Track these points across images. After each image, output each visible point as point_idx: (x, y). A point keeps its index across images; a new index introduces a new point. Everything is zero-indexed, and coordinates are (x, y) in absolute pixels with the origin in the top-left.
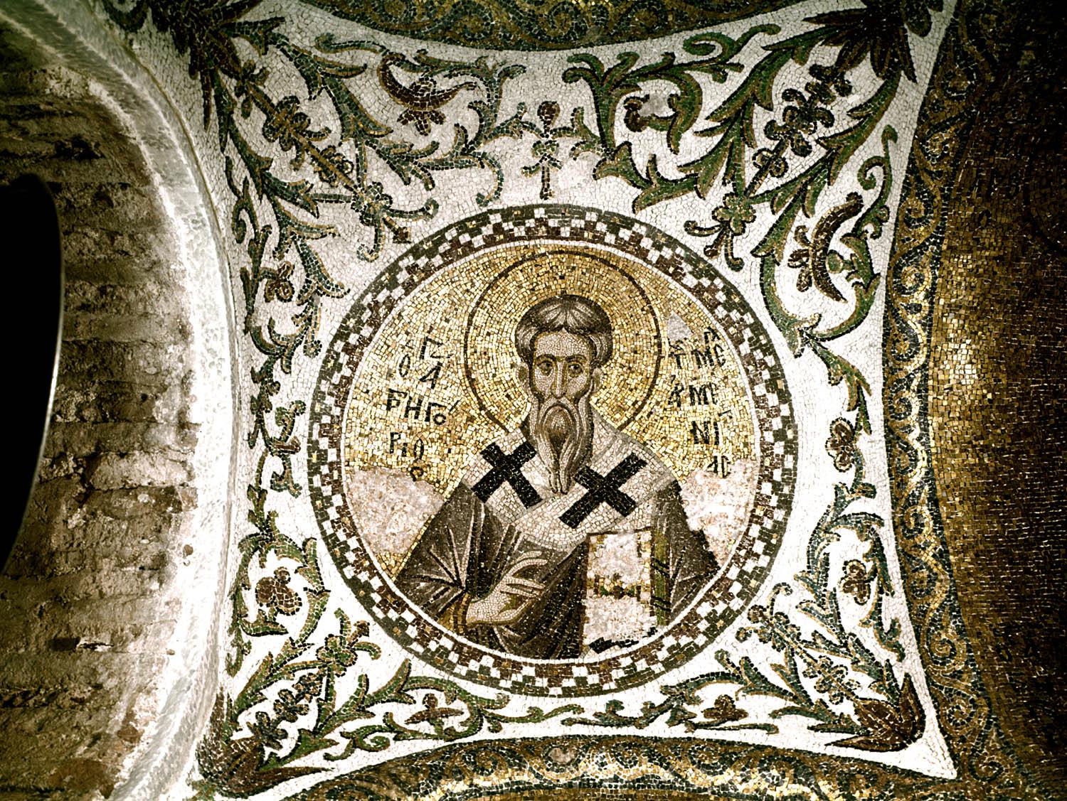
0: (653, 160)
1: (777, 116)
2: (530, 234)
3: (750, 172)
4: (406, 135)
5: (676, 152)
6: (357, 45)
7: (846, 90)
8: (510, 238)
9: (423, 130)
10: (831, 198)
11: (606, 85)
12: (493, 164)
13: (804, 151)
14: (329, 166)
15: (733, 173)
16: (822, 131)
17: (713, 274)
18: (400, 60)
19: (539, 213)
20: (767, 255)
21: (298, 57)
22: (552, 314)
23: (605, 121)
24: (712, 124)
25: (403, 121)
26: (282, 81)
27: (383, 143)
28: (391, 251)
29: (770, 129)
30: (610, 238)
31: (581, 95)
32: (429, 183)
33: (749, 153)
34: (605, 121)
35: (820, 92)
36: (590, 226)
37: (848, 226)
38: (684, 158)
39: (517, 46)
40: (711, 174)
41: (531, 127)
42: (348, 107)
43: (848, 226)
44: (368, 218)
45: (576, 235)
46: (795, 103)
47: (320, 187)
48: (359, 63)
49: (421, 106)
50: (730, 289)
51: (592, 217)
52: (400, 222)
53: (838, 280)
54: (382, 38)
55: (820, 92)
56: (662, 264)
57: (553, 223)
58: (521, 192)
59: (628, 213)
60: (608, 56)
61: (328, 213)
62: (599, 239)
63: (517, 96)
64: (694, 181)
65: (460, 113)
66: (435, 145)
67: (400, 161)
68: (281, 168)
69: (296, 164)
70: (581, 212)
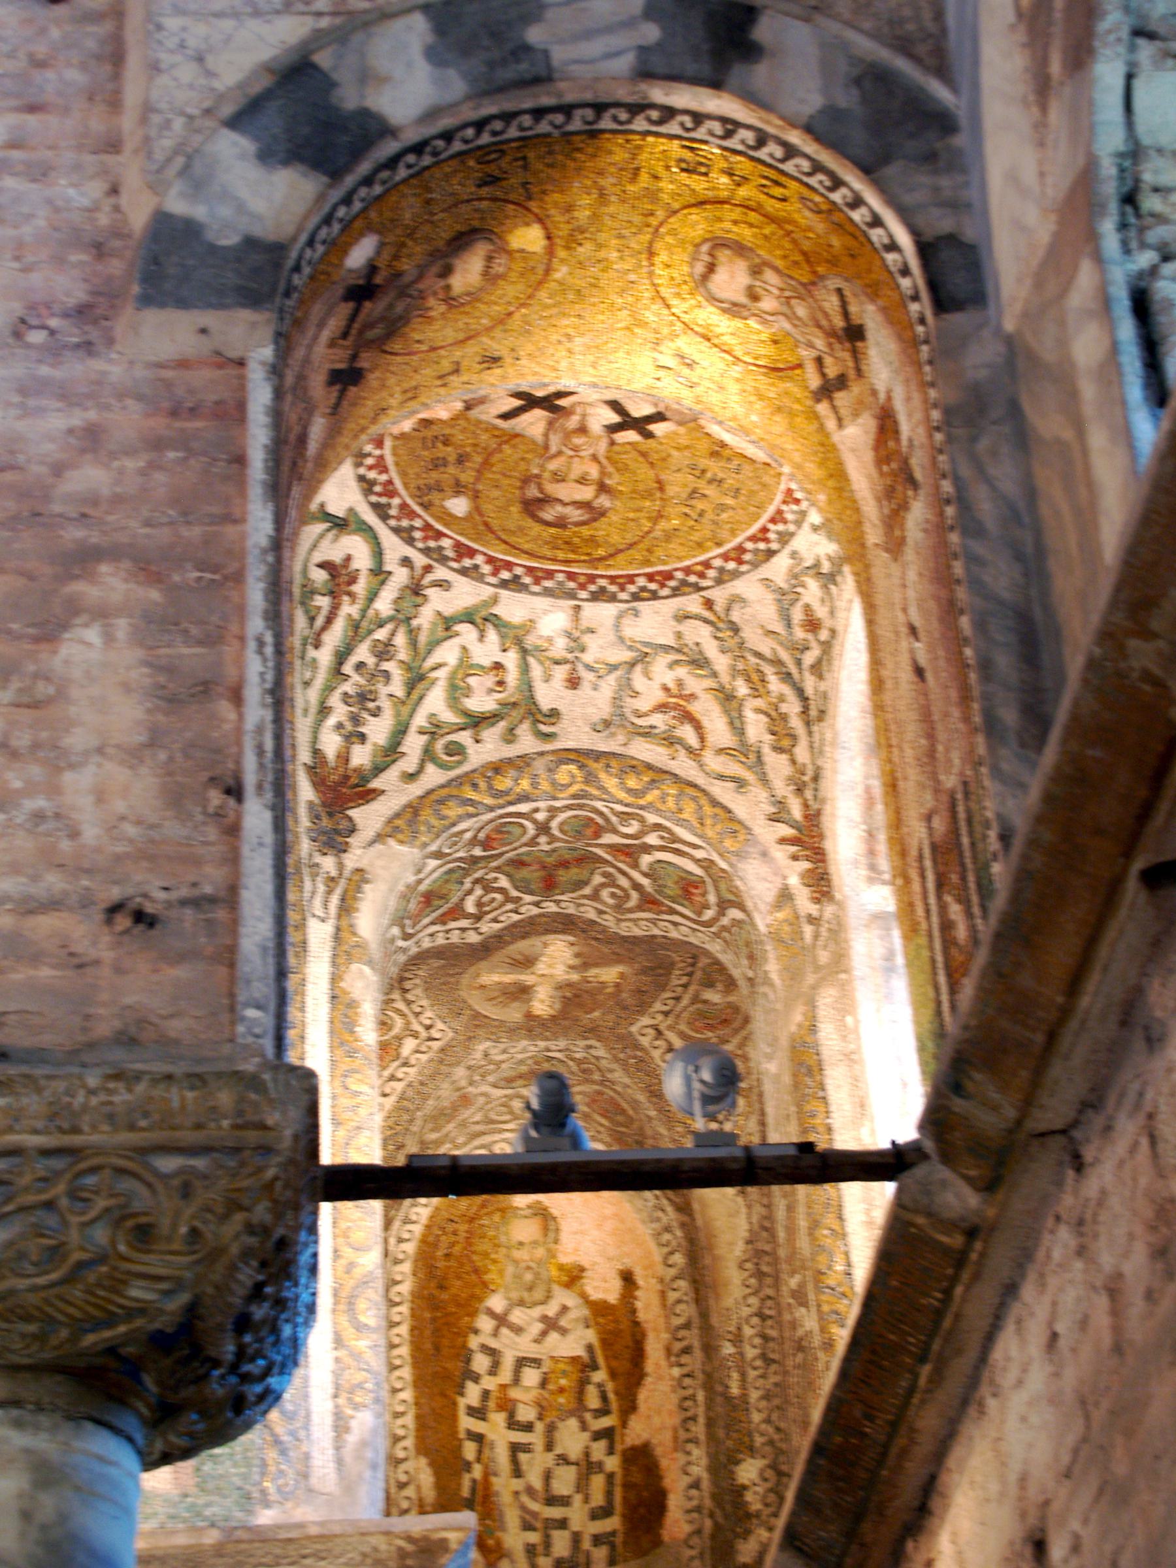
0: (482, 638)
1: (383, 690)
2: (592, 579)
3: (400, 640)
4: (696, 684)
5: (464, 649)
6: (721, 777)
7: (339, 726)
8: (612, 579)
9: (680, 683)
10: (334, 636)
11: (528, 711)
12: (621, 639)
13: (360, 666)
14: (758, 685)
15: (413, 643)
16: (347, 687)
17: (426, 551)
18: (690, 750)
19: (583, 594)
20: (380, 573)
21: (764, 780)
22: (575, 514)
23: (525, 669)
24: (434, 674)
25: (692, 697)
26: (778, 766)
27: (710, 683)
28: (719, 595)
29: (387, 675)
30: (519, 571)
31: (548, 695)
32: (679, 635)
33: (403, 655)
34: (525, 669)
35: (355, 719)
36: (537, 581)
37: (320, 621)
38: (456, 641)
39: (598, 756)
40: (432, 631)
41: (589, 668)
42: (737, 727)
43: (320, 621)
44: (735, 629)
45: (550, 574)
46: (371, 705)
47: (769, 670)
48: (722, 758)
49: (678, 706)
50: (410, 541)
51: (536, 589)
52: (707, 614)
53: (320, 576)
54: (701, 780)
55: (355, 719)
56: (472, 553)
57: (572, 585)
58: (601, 614)
59: (504, 593)
60: (527, 743)
61: (765, 646)
62: (530, 570)
63: (596, 699)
64: (448, 624)
65: (649, 689)
66: (672, 665)
67: (699, 662)
68: (792, 707)
69: (782, 698)
70: (548, 592)
